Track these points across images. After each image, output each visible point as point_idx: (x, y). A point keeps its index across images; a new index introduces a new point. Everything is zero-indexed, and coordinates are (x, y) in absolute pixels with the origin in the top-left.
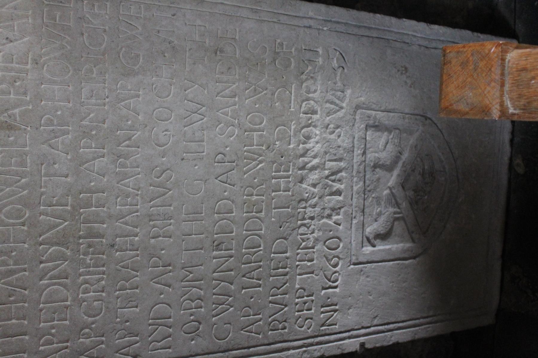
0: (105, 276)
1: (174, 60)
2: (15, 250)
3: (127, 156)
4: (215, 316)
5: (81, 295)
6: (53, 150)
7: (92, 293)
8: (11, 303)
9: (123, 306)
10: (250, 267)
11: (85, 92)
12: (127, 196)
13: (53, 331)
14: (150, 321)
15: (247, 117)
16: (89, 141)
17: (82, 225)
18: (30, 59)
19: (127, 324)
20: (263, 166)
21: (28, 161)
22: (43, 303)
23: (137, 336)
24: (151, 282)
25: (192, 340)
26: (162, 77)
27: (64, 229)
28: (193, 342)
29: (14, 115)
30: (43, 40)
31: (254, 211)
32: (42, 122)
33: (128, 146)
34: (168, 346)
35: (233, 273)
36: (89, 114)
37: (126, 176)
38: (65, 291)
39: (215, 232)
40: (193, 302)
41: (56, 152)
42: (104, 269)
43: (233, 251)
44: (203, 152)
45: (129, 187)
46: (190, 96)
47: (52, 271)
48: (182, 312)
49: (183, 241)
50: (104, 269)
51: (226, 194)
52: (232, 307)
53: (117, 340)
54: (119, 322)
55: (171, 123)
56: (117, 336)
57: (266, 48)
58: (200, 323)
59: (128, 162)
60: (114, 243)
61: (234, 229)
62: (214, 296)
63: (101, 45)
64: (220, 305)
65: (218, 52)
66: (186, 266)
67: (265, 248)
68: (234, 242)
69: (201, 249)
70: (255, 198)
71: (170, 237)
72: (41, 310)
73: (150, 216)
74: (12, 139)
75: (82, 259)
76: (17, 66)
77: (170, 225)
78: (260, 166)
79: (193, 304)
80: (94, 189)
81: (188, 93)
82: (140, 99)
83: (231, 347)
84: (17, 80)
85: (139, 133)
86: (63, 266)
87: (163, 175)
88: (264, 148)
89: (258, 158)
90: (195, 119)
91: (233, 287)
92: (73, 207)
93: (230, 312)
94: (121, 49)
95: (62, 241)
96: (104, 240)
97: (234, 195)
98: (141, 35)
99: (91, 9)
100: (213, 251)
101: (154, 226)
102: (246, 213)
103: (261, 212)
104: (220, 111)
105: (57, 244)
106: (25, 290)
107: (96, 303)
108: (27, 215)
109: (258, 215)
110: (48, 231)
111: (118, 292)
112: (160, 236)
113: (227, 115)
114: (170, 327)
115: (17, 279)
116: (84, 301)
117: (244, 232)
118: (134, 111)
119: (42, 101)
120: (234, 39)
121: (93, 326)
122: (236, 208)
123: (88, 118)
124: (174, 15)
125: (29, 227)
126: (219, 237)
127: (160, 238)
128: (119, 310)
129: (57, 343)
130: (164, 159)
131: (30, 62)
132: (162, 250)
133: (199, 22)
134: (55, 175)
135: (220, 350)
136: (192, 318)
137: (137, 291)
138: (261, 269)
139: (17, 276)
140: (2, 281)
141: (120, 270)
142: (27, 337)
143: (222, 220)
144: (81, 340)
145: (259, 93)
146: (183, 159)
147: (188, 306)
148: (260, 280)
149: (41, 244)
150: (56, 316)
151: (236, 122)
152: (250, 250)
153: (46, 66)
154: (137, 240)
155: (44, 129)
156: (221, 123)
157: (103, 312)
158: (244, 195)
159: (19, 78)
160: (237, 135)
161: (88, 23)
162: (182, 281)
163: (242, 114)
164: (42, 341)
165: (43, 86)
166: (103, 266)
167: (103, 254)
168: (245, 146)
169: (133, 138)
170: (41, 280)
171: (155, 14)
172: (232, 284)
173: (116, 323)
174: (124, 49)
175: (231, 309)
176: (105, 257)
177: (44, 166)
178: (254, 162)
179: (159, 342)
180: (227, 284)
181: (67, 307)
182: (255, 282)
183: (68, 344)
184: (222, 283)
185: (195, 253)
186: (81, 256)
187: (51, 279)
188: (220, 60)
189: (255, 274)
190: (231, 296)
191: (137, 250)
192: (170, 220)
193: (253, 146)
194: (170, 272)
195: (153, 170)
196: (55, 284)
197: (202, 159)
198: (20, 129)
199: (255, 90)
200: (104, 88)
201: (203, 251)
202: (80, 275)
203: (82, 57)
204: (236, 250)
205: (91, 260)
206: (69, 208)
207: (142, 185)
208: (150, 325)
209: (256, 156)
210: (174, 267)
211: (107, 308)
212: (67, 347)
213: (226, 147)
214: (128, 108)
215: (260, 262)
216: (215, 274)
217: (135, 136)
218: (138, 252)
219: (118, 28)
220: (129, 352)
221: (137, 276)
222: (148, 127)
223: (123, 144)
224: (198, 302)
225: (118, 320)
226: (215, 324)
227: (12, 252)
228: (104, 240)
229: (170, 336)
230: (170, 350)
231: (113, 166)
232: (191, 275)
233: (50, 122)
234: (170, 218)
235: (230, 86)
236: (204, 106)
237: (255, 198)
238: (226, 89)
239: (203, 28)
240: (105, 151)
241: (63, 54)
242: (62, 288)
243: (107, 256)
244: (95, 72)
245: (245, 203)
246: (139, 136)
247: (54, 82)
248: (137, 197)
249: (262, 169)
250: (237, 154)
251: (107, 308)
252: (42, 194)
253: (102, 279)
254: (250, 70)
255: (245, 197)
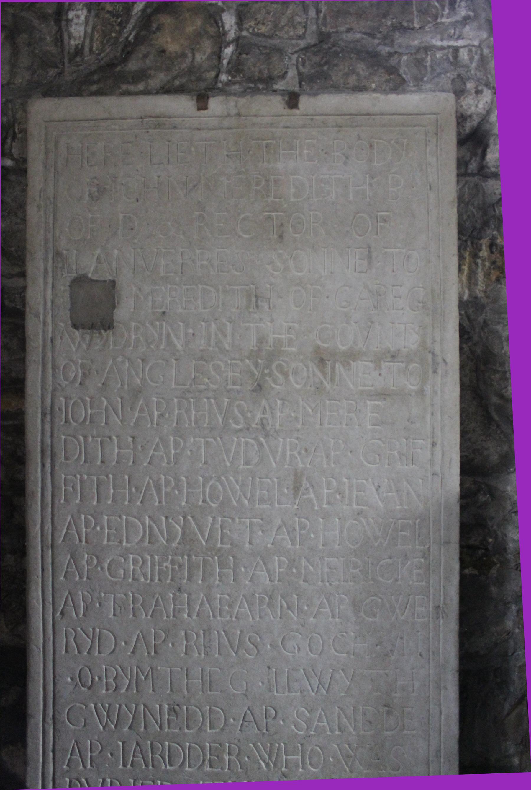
0: (148, 581)
1: (374, 656)
2: (179, 493)
3: (271, 605)
4: (95, 707)
5: (131, 556)
6: (275, 529)
7: (132, 567)
8: (130, 489)
9: (117, 601)
10: (147, 752)
11: (333, 561)
12: (230, 606)
13: (98, 528)
14: (98, 630)
15: (318, 746)
16: (286, 565)
17: (202, 558)
18: (362, 507)
19: (98, 605)
20: (262, 768)
21: (265, 506)
22: (127, 520)
23: (84, 615)
24: (138, 632)
25: (72, 679)
26: (355, 643)
27: (198, 540)
28: (69, 680)
29: (308, 493)
30: (381, 520)
31: (212, 757)
32: (303, 520)
33: (281, 607)
34: (69, 650)
35: (142, 729)
36: (312, 566)
37: (251, 604)
38: (136, 541)
39: (190, 707)
40: (114, 680)
41: (274, 533)
42: (156, 581)
43: (166, 730)
44: (277, 692)
45: (239, 607)
46: (337, 676)
47: (158, 527)
48: (104, 667)
49: (181, 668)
50: (156, 581)
51: (232, 720)
52: (104, 728)
53: (82, 593)
54: (100, 596)
55: (307, 654)
56: (86, 593)
57: (398, 770)
58: (89, 688)
59: (265, 606)
60: (182, 591)
61: (191, 731)
62: (118, 706)
63: (382, 576)
64: (108, 713)
65: (387, 708)
66: (154, 671)
67: (167, 772)
68: (177, 731)
69: (171, 690)
70: (227, 758)
71: (186, 653)
72: (120, 517)
73: (209, 630)
74: (286, 491)
75: (168, 559)
76: (355, 496)
77: (199, 654)
78: (263, 764)
79: (111, 680)
80: (238, 570)
81: (340, 674)
82: (330, 619)
83: (57, 727)
84: (341, 495)
85: (295, 618)
86: (162, 539)
87: (252, 646)
88: (283, 769)
89: (272, 762)
90: (312, 682)
91: (126, 729)
92: (220, 549)
93: (98, 726)
94: (380, 598)
95: (187, 538)
96: (185, 581)
97: (230, 731)
98: (397, 618)
99: (416, 566)
100: (168, 705)
101: (198, 635)
102: (210, 747)
103: (211, 766)
104: (323, 713)
105: (184, 533)
106: (141, 502)
107: (122, 571)
108: (213, 505)
109: (207, 762)
110: (197, 525)
111: (131, 595)
112: (187, 641)
113: (318, 721)
114: (88, 653)
115: (152, 495)
116: (125, 560)
117: (188, 744)
118: (318, 613)
119: (323, 519)
120: (404, 729)
121: (99, 569)
122: (216, 733)
123: (308, 564)
124: (421, 655)
125: (201, 506)
126: (184, 712)
127: (185, 642)
128: (113, 596)
129: (86, 532)
130: (269, 646)
131: (360, 507)
132: (173, 644)
133: (417, 684)
134: (251, 532)
135: (56, 713)
136: (97, 678)
137: (131, 616)
138: (144, 767)
139: (155, 494)
140: (151, 481)
141: (153, 597)
142: (95, 503)
143: (202, 715)
144: (86, 556)
145: (346, 762)
146: (269, 668)
147: (109, 674)
148: (132, 765)
149: (184, 518)
150: (113, 531)
151: (312, 733)
152: (167, 752)
153: (357, 522)
154: (184, 617)
155: (295, 522)
156: (309, 712)
157: (112, 579)
158: (230, 743)
159: (343, 497)
160: (297, 734)
161: (402, 563)
162: (138, 667)
163: (321, 739)
164: (89, 517)
165: (337, 520)
166: (159, 580)
167: (172, 580)
168: (285, 744)
169: (290, 612)
170: (149, 517)
171: (419, 633)
172: (130, 728)
173: (99, 593)
174: (380, 600)
175: (101, 727)
176: (168, 581)
177: (261, 521)
178: (267, 756)
179: (74, 640)
180: (131, 721)
181: (121, 542)
182: (129, 759)
183: (84, 543)
184: (132, 716)
185: (167, 683)
186: (170, 557)
187: (150, 527)
188: (379, 711)
189: (139, 759)
190: (115, 727)
191: (174, 616)
192: (204, 654)
193: (286, 755)
194: (148, 653)
195: (258, 634)
196: (145, 532)
197: (270, 690)
198: (295, 498)
199: (349, 756)
200: (339, 581)
201: (168, 692)
202: (152, 556)
203: (368, 558)
204: (168, 733)
205: (166, 567)
206: (219, 545)
207: (241, 621)
208: (94, 630)
209: (274, 759)
210: (153, 658)
211: (116, 584)
212: (80, 541)
213: (283, 720)
214: (321, 606)
215: (153, 766)
216: (142, 706)
217: (292, 614)
218: (171, 618)
219: (400, 594)
220: (68, 606)
221: (146, 616)
222: (301, 628)
223: (283, 602)
224: (112, 686)
225: (103, 595)
226: (86, 706)
227: (178, 490)
228: (185, 581)
229: (79, 652)
230: (64, 652)
231: (261, 591)
232: (143, 678)
233: (303, 527)
234: (206, 654)
235: (350, 724)
236: (327, 692)
237: (227, 758)
238: (347, 720)
239: (411, 689)
240: (276, 582)
241: (369, 538)
242: (140, 538)
243: (170, 584)
244: (354, 571)
245: (220, 744)
246: (292, 619)
247: (341, 531)
248: (229, 616)
249: (260, 767)
250: (276, 733)
251: (116, 584)
252: (233, 519)
253: (146, 579)
254: (371, 749)
255: (227, 745)
